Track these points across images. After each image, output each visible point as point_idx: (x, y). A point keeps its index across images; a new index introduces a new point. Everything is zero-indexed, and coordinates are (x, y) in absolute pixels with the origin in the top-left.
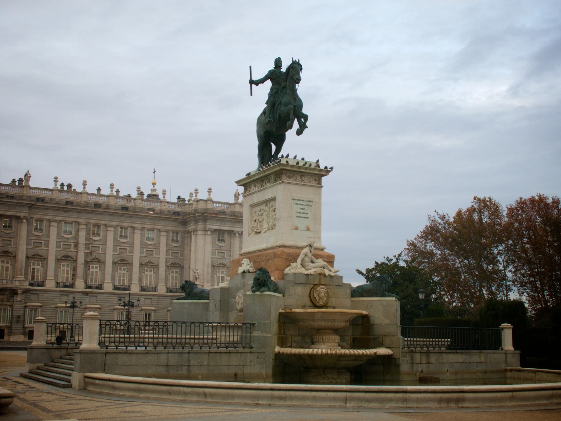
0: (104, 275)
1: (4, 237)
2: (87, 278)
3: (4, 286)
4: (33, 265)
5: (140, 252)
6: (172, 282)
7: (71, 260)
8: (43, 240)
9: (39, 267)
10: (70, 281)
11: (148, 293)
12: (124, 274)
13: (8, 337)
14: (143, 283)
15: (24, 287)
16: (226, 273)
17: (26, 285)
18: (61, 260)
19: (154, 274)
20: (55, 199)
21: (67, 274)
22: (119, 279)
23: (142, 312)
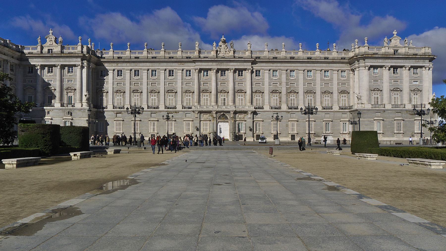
2: (288, 103)
6: (343, 103)
10: (278, 105)
11: (327, 110)
12: (311, 99)
14: (323, 104)
15: (252, 110)
16: (380, 95)
17: (252, 109)
21: (277, 101)
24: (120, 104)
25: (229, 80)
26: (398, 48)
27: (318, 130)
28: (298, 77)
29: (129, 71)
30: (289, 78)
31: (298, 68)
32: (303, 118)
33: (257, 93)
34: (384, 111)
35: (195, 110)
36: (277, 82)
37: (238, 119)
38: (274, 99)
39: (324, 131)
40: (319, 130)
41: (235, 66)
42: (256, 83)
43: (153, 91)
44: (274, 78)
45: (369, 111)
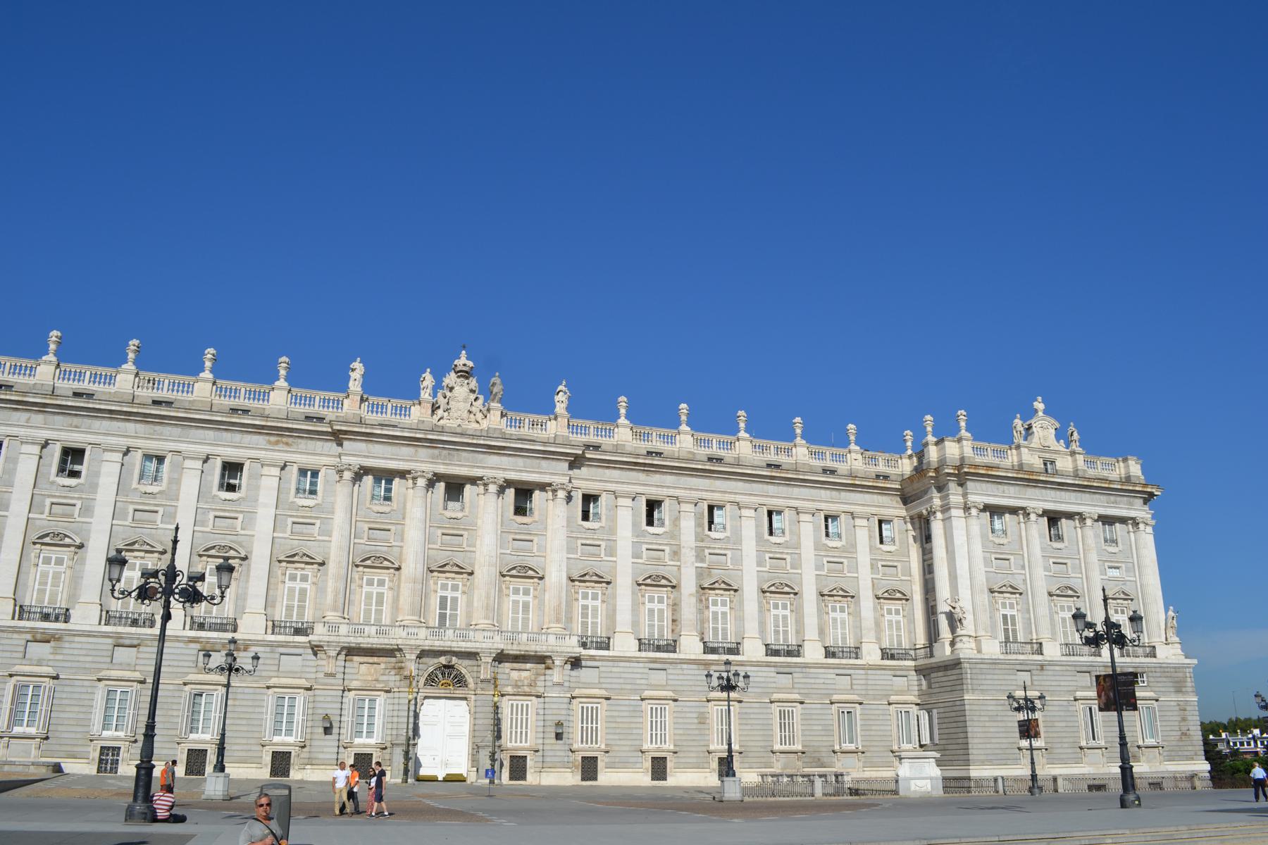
0: (740, 619)
1: (516, 533)
3: (523, 648)
4: (583, 598)
5: (816, 566)
6: (891, 636)
7: (666, 586)
8: (603, 540)
9: (598, 603)
11: (844, 661)
12: (785, 617)
13: (535, 775)
14: (827, 639)
15: (569, 650)
17: (572, 646)
18: (646, 585)
19: (851, 617)
20: (624, 445)
23: (834, 707)
25: (479, 522)
26: (1053, 456)
29: (36, 449)
31: (738, 498)
33: (584, 581)
34: (1042, 666)
35: (326, 639)
36: (660, 544)
38: (651, 611)
40: (820, 738)
42: (584, 542)
43: (136, 547)
45: (997, 666)
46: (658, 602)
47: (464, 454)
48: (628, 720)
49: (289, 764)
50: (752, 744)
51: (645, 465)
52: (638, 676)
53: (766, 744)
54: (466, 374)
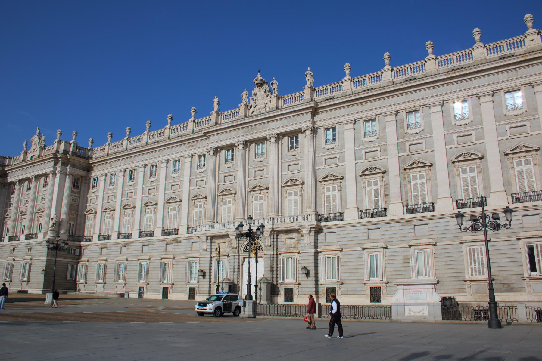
0: (434, 187)
1: (290, 162)
10: (382, 205)
12: (473, 178)
21: (376, 195)
22: (464, 190)
23: (521, 241)
24: (108, 232)
27: (503, 269)
28: (429, 125)
30: (406, 131)
31: (427, 101)
32: (452, 235)
33: (327, 181)
36: (375, 147)
37: (283, 250)
39: (525, 271)
41: (277, 128)
42: (326, 157)
44: (367, 139)
46: (374, 185)
47: (259, 126)
48: (355, 263)
49: (195, 294)
50: (446, 275)
51: (357, 99)
52: (361, 235)
53: (459, 275)
54: (261, 85)
